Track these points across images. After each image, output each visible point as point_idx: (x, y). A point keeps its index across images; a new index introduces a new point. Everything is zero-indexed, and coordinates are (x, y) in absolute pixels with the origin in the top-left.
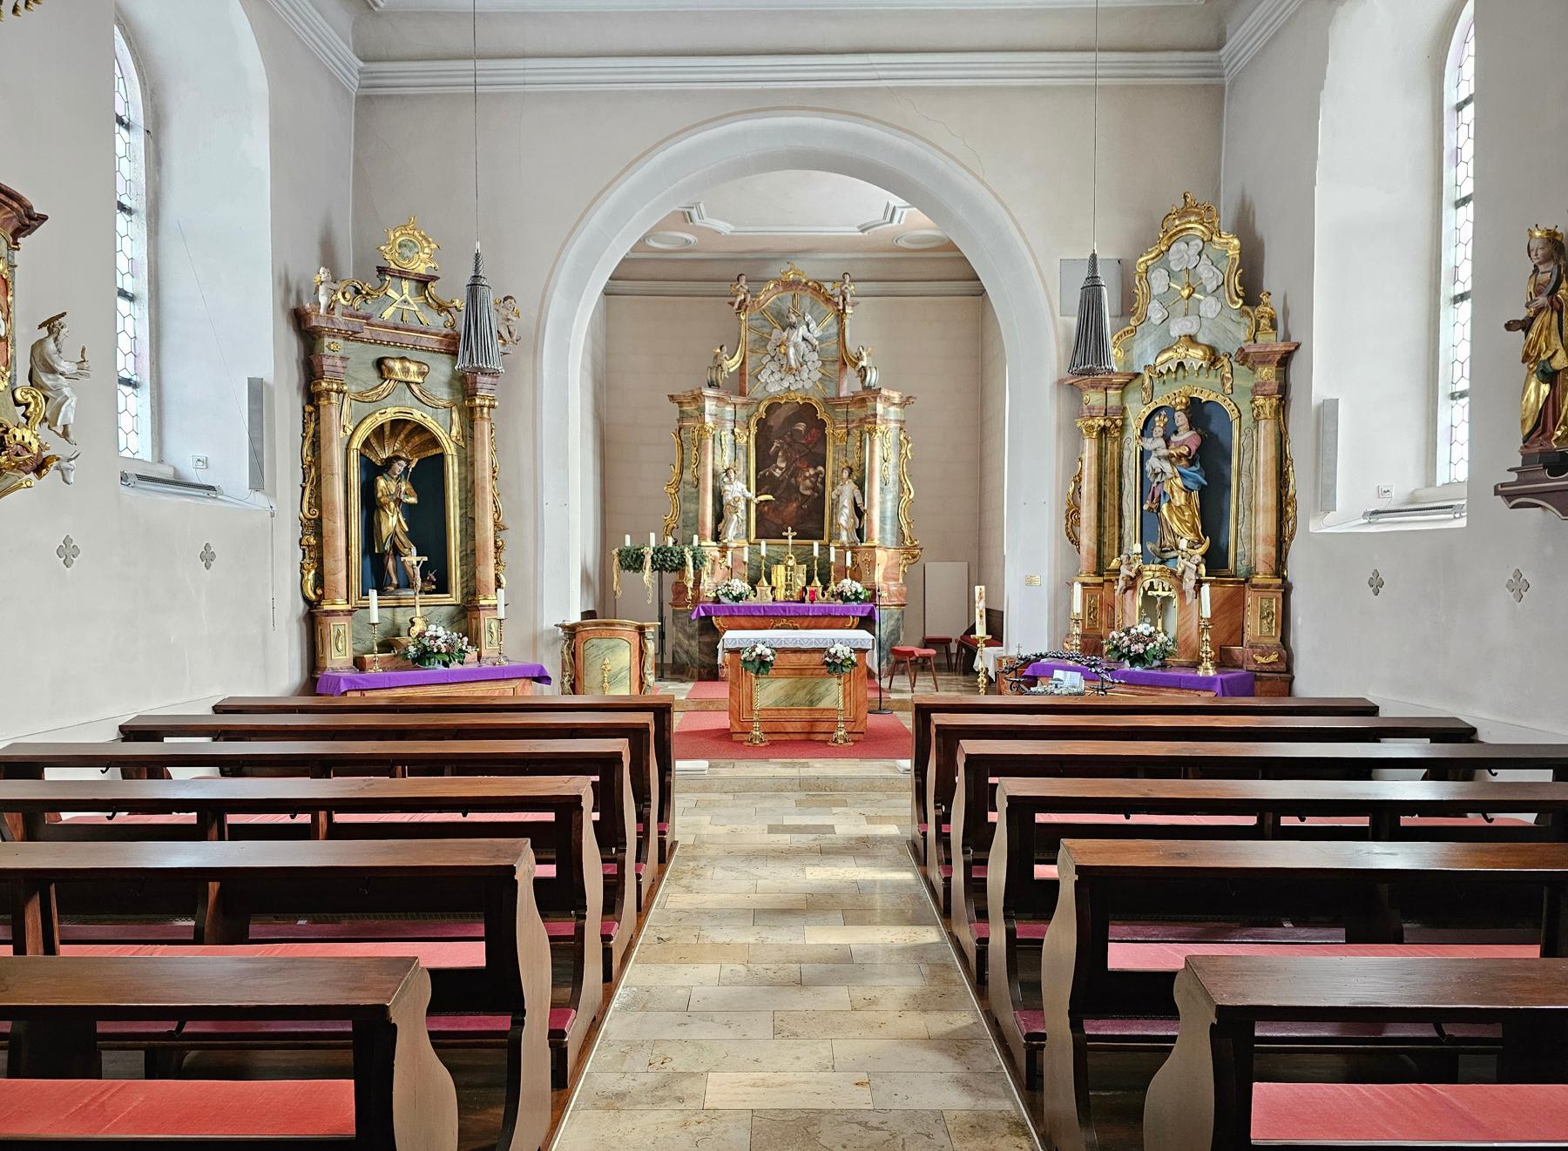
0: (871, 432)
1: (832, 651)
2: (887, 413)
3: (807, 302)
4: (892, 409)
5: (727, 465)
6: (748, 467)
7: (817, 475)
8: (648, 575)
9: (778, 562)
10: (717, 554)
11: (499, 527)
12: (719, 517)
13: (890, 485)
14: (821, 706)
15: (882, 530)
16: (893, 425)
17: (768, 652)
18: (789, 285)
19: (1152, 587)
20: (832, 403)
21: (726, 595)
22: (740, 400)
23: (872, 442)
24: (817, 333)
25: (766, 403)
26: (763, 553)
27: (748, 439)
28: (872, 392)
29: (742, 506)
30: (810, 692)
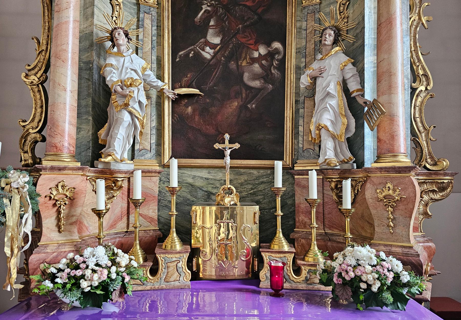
7: (271, 55)
9: (208, 198)
26: (174, 183)
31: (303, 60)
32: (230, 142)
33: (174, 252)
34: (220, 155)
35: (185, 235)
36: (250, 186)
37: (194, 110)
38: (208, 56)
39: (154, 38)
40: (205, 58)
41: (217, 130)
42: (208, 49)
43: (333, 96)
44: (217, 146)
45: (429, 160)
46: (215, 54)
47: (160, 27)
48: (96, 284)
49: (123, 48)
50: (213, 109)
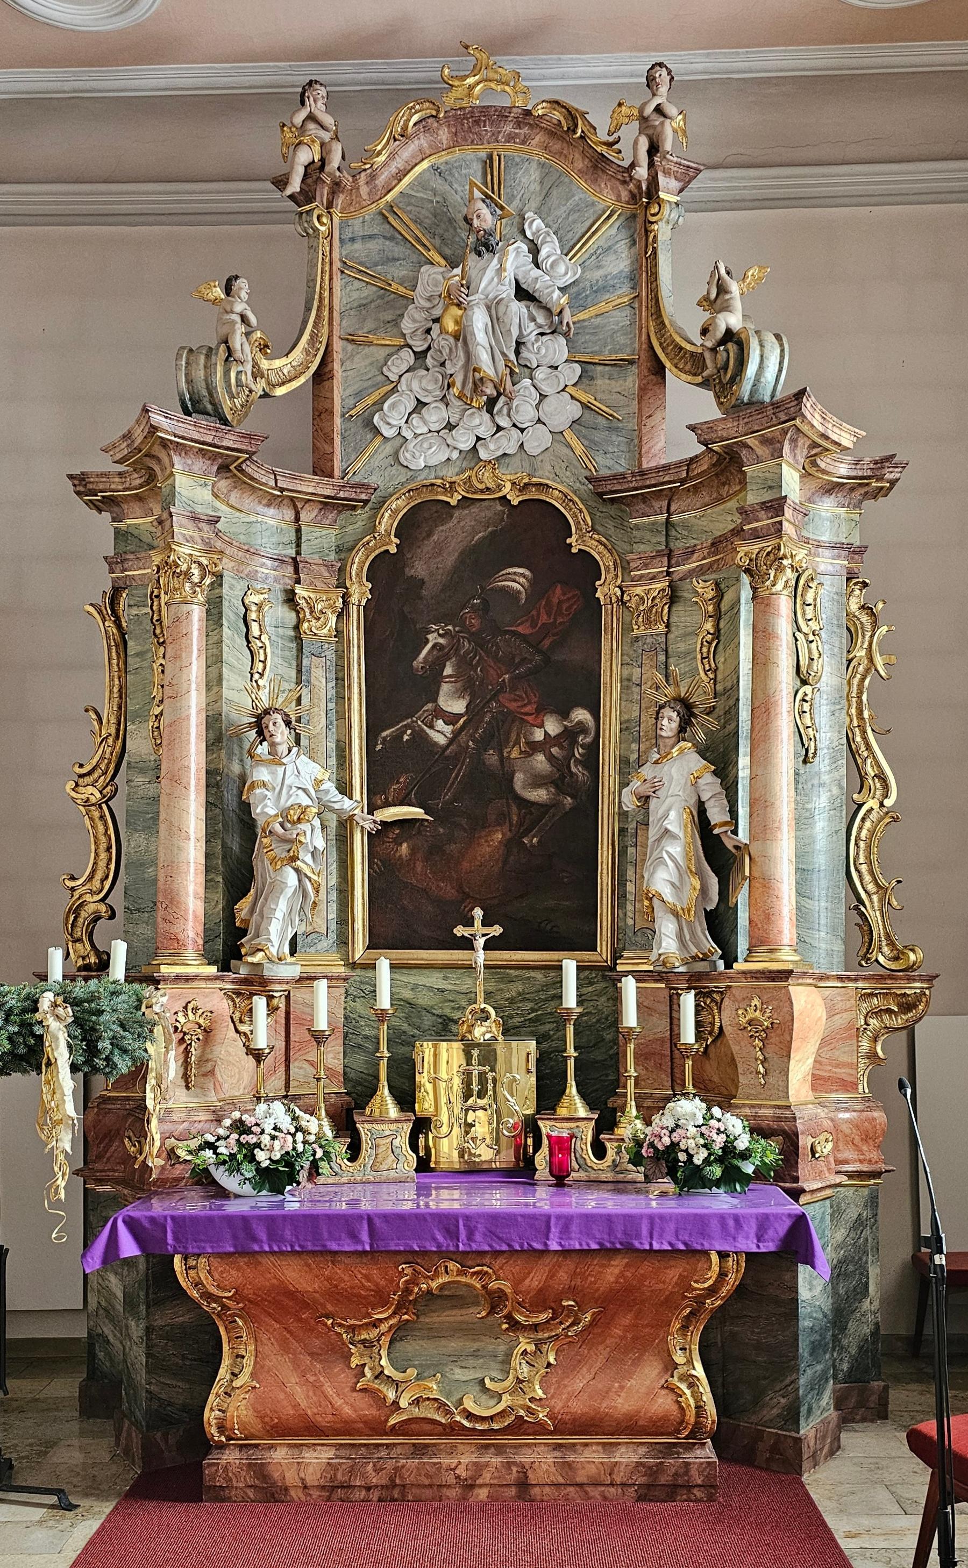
6: (342, 715)
7: (570, 735)
9: (444, 1029)
10: (223, 1006)
12: (236, 874)
13: (822, 764)
15: (802, 916)
18: (471, 122)
21: (231, 1163)
22: (310, 485)
24: (566, 272)
26: (384, 1002)
27: (338, 616)
29: (316, 838)
31: (634, 746)
32: (484, 924)
33: (384, 1122)
34: (467, 944)
35: (406, 1097)
36: (530, 1005)
37: (413, 851)
38: (441, 740)
39: (332, 706)
40: (436, 744)
41: (460, 889)
42: (440, 724)
43: (674, 837)
44: (460, 931)
45: (886, 949)
46: (456, 734)
47: (341, 680)
48: (277, 1156)
49: (282, 749)
50: (453, 848)
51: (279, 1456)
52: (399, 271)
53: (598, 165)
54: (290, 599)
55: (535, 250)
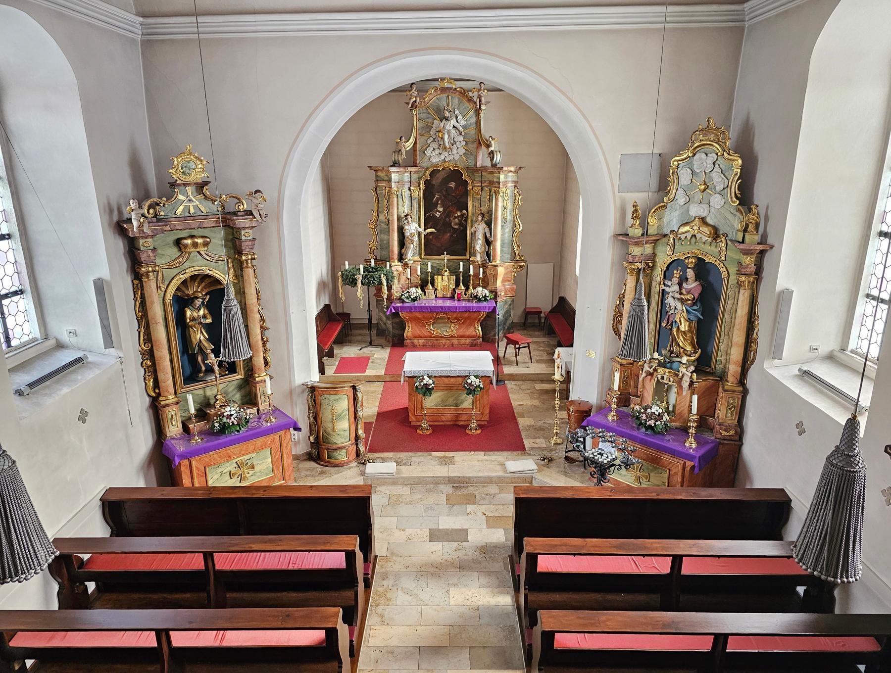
0: (497, 193)
1: (469, 381)
2: (507, 178)
3: (456, 101)
4: (510, 174)
5: (406, 211)
6: (419, 211)
7: (462, 215)
8: (360, 290)
10: (400, 269)
11: (263, 329)
12: (402, 244)
13: (508, 223)
14: (463, 406)
16: (510, 184)
17: (431, 382)
19: (662, 378)
20: (473, 170)
22: (413, 169)
23: (497, 199)
24: (463, 122)
25: (431, 170)
27: (419, 193)
28: (496, 168)
29: (416, 238)
30: (456, 399)
47: (419, 204)
51: (416, 341)
52: (429, 120)
53: (470, 100)
54: (410, 189)
55: (457, 117)
